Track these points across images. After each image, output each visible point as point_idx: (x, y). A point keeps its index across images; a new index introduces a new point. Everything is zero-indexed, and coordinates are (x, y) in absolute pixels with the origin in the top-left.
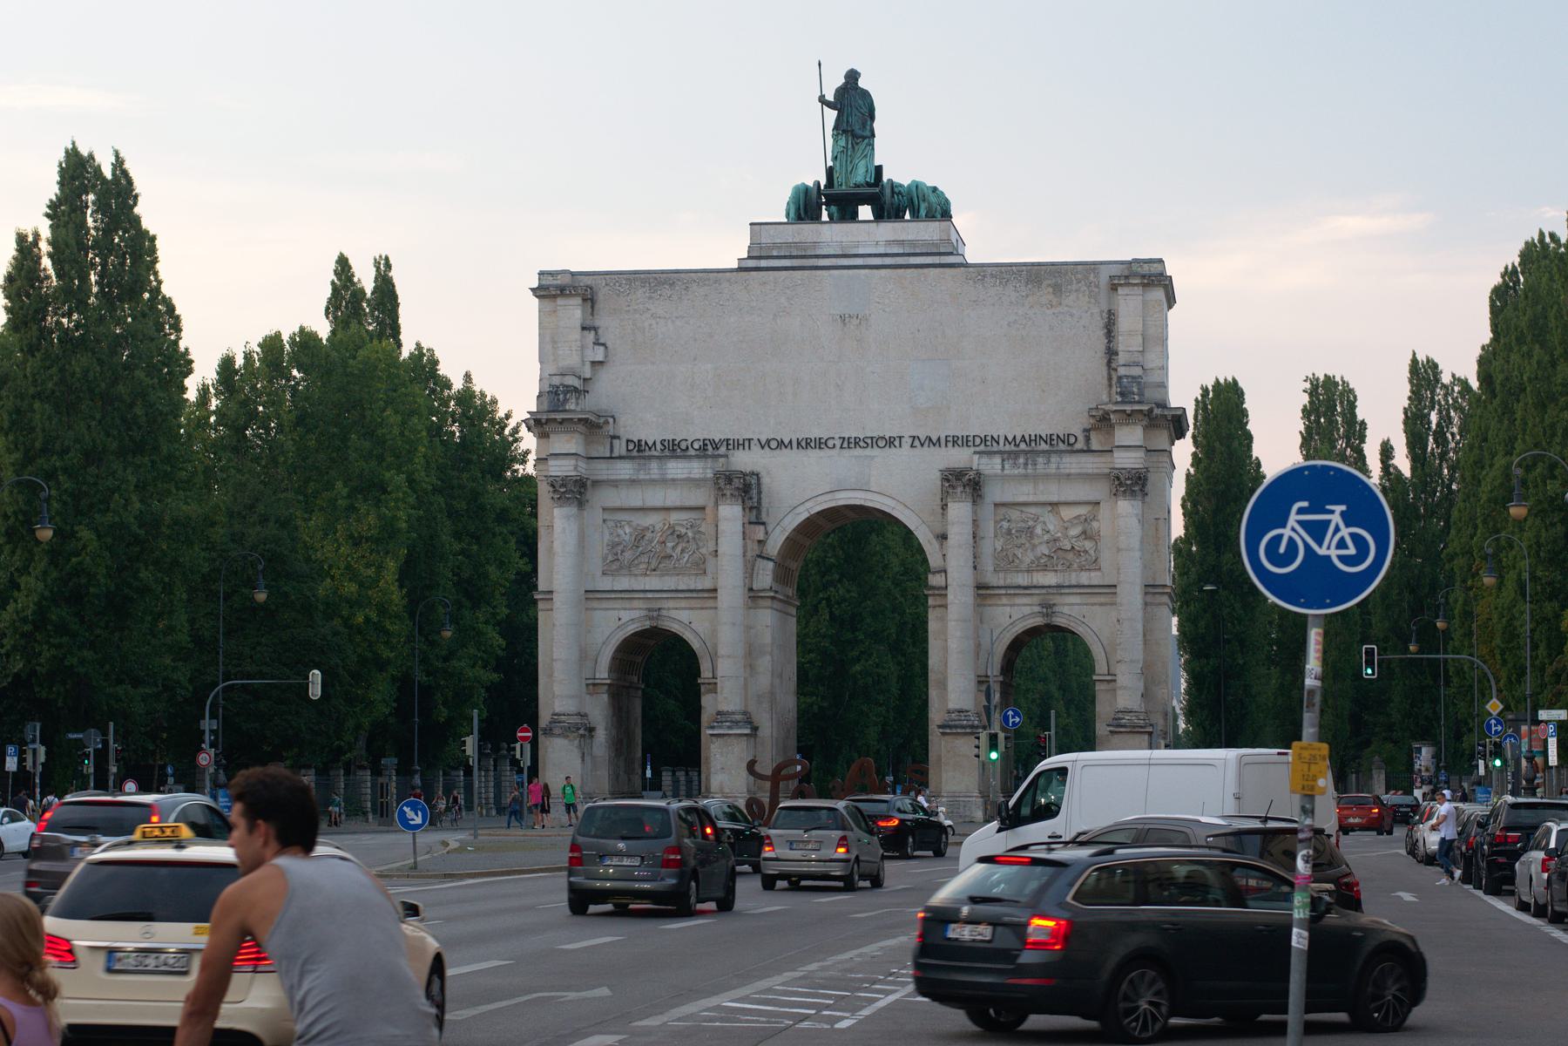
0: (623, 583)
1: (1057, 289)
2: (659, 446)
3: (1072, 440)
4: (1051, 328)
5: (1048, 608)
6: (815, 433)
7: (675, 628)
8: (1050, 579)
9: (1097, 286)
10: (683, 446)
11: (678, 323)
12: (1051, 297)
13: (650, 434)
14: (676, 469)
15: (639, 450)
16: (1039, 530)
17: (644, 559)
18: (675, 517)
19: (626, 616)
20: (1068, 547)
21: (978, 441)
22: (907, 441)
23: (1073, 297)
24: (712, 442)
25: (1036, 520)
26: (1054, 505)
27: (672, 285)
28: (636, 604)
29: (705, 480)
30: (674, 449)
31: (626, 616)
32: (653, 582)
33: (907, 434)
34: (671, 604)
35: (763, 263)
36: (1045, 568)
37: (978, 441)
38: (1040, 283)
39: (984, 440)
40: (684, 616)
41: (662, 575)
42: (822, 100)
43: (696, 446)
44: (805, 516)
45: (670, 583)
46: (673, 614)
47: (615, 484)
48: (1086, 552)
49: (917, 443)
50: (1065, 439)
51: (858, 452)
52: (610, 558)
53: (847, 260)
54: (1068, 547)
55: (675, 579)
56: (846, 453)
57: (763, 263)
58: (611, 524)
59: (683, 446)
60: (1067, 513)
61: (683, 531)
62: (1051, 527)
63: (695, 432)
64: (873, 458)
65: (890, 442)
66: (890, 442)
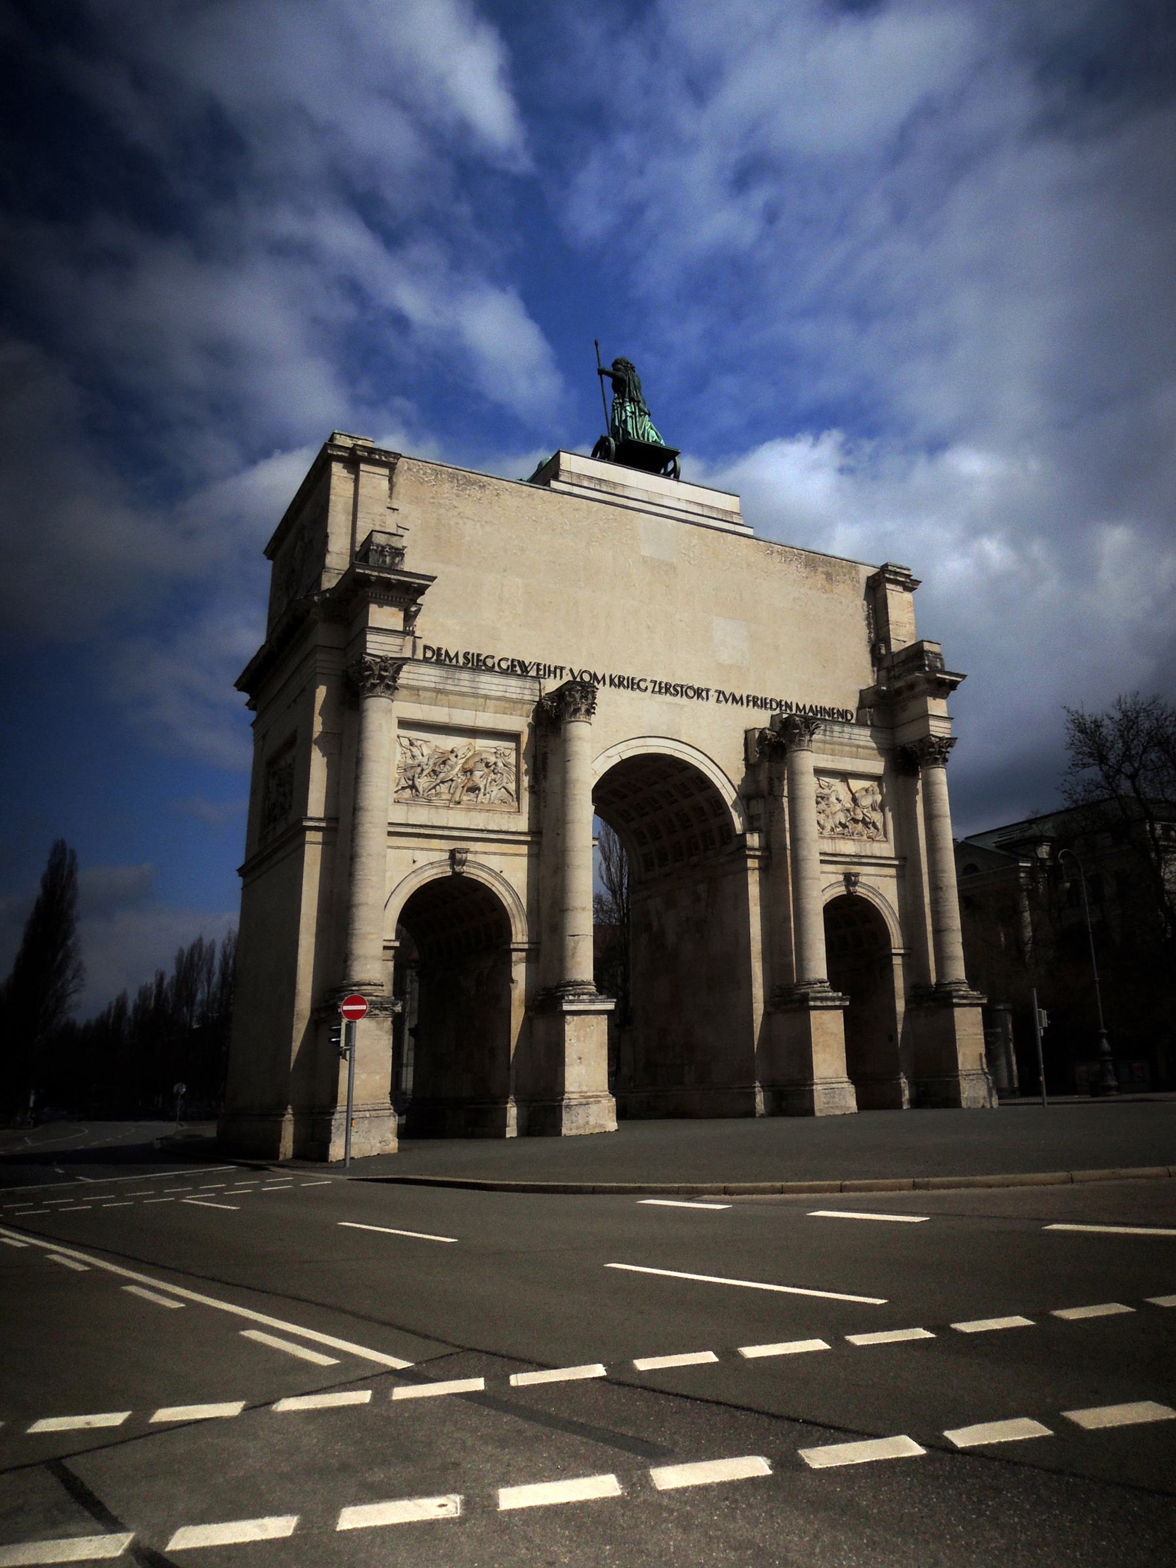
0: (421, 815)
1: (829, 576)
2: (461, 660)
3: (849, 717)
4: (827, 610)
5: (850, 880)
6: (628, 673)
7: (483, 877)
8: (848, 847)
9: (858, 582)
10: (489, 662)
11: (488, 528)
12: (825, 582)
13: (454, 645)
14: (490, 684)
15: (439, 658)
16: (833, 799)
17: (443, 788)
18: (481, 744)
19: (423, 858)
20: (860, 817)
21: (774, 706)
22: (713, 695)
23: (841, 586)
24: (522, 664)
25: (829, 787)
26: (844, 776)
27: (483, 487)
28: (435, 843)
29: (521, 702)
30: (477, 664)
31: (423, 858)
32: (457, 818)
33: (714, 687)
34: (478, 846)
35: (576, 490)
36: (843, 836)
37: (774, 706)
38: (815, 569)
39: (779, 704)
40: (494, 862)
41: (469, 810)
42: (601, 372)
43: (504, 665)
44: (616, 760)
45: (478, 820)
46: (482, 859)
47: (415, 690)
48: (874, 825)
49: (721, 698)
50: (843, 714)
51: (668, 697)
52: (403, 783)
53: (651, 508)
54: (860, 817)
55: (484, 815)
56: (657, 695)
57: (576, 490)
58: (406, 742)
59: (489, 662)
60: (856, 785)
61: (492, 759)
62: (841, 797)
63: (504, 649)
64: (682, 707)
65: (698, 693)
66: (698, 693)
